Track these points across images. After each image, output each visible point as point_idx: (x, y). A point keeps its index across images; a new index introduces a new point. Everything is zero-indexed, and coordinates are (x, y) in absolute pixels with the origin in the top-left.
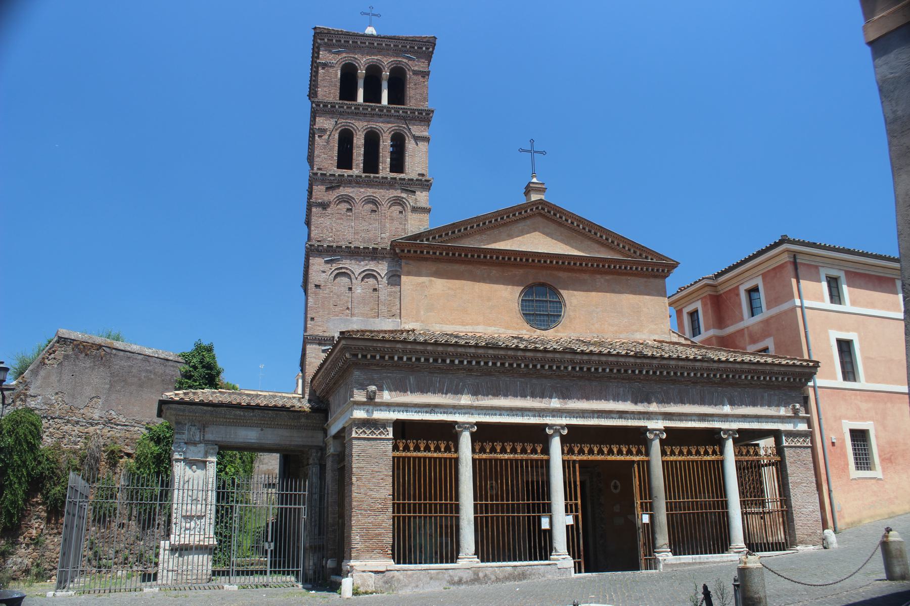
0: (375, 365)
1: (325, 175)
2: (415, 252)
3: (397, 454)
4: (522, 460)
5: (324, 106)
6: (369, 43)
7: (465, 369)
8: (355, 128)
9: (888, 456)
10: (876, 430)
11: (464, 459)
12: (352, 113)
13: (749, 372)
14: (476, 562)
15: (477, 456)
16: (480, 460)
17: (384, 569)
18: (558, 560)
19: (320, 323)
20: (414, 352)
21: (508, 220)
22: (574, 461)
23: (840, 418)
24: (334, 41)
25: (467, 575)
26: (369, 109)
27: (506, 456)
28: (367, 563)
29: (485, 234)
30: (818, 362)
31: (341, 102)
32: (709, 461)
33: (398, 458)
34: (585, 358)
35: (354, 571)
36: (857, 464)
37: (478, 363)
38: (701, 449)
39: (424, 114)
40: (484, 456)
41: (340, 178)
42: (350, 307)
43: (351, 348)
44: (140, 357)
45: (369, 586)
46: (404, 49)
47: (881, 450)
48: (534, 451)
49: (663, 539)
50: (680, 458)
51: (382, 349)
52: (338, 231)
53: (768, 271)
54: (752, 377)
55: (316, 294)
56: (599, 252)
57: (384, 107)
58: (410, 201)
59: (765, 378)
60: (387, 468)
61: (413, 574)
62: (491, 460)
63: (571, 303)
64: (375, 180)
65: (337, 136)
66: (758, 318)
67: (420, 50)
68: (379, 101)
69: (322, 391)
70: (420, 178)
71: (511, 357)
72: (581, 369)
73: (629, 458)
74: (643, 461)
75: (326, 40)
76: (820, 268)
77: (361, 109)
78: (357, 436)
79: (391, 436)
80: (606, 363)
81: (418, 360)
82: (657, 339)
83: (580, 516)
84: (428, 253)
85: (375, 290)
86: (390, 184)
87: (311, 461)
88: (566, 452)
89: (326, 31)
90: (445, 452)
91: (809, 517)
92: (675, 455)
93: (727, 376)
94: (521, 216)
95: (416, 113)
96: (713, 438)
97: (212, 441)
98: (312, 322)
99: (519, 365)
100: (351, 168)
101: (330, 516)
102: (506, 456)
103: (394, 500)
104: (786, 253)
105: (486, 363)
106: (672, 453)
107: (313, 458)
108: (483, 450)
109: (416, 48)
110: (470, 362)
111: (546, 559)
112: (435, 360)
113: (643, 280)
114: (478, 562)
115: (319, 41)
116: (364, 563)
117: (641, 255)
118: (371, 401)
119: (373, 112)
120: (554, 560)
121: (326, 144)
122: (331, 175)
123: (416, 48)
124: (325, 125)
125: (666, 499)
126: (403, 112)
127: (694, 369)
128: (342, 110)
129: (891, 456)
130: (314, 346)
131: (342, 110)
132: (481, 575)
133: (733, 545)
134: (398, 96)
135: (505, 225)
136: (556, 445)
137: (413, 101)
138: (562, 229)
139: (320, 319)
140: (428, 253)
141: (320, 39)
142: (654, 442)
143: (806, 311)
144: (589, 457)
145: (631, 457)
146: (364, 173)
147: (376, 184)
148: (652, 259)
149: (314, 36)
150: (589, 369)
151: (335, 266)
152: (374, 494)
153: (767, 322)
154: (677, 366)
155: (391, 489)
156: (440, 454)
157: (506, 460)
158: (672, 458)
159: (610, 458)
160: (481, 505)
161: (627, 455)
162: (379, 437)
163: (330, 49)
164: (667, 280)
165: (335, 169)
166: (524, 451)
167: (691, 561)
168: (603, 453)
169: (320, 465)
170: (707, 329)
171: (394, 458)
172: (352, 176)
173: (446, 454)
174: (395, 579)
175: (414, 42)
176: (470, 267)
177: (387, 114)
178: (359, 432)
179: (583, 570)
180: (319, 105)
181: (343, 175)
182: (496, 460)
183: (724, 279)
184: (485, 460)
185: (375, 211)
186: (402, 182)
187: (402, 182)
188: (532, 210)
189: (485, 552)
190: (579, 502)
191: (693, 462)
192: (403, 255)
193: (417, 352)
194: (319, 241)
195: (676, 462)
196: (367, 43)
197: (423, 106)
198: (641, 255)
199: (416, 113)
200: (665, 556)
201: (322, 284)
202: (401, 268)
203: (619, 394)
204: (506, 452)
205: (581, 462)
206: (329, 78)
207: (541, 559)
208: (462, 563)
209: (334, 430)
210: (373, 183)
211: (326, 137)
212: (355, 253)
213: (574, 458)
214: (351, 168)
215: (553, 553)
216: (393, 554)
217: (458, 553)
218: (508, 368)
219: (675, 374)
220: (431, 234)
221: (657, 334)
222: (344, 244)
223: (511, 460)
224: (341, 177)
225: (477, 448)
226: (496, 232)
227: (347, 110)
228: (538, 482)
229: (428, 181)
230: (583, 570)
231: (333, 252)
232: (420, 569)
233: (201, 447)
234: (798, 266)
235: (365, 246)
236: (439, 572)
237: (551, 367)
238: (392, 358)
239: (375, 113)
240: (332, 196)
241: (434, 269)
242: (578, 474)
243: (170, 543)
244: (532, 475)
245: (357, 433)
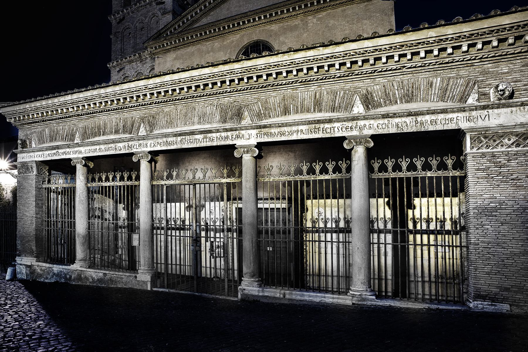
213: (163, 183)
225: (90, 178)
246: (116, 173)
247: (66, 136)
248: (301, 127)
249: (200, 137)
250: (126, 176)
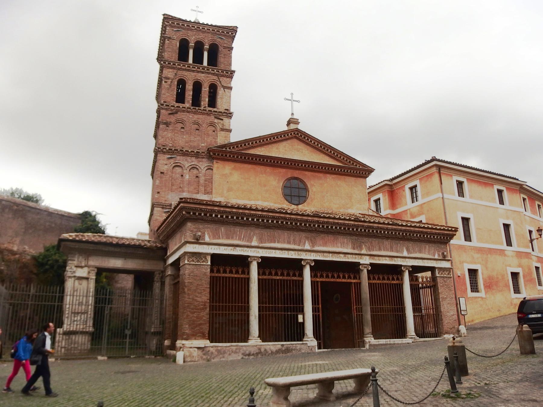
0: (201, 219)
2: (222, 155)
3: (213, 275)
4: (287, 280)
5: (169, 63)
7: (255, 224)
8: (188, 79)
9: (488, 284)
10: (482, 270)
11: (253, 279)
12: (186, 69)
13: (419, 232)
14: (259, 342)
15: (260, 277)
16: (262, 279)
17: (203, 346)
18: (308, 341)
19: (163, 196)
20: (225, 212)
21: (277, 140)
22: (317, 282)
23: (463, 262)
25: (254, 350)
26: (196, 68)
27: (278, 278)
28: (192, 342)
30: (457, 228)
31: (179, 62)
32: (395, 284)
33: (213, 277)
34: (326, 220)
35: (185, 348)
36: (471, 289)
37: (263, 220)
38: (390, 277)
40: (265, 277)
41: (177, 108)
42: (181, 186)
43: (186, 208)
44: (46, 213)
45: (193, 357)
46: (218, 33)
47: (485, 281)
48: (294, 275)
49: (368, 329)
50: (378, 282)
51: (205, 210)
52: (175, 140)
53: (423, 177)
54: (420, 236)
55: (161, 177)
56: (329, 161)
57: (205, 67)
58: (220, 125)
59: (427, 236)
60: (206, 283)
61: (221, 349)
62: (269, 279)
63: (312, 190)
64: (199, 111)
65: (176, 83)
66: (416, 204)
67: (228, 35)
68: (202, 63)
69: (164, 237)
70: (226, 111)
71: (282, 218)
72: (323, 226)
73: (349, 281)
74: (357, 283)
76: (453, 176)
78: (188, 263)
79: (209, 263)
80: (338, 223)
81: (227, 217)
82: (361, 213)
83: (321, 315)
84: (230, 156)
85: (197, 177)
86: (209, 114)
87: (155, 279)
88: (313, 276)
89: (170, 17)
90: (242, 274)
91: (451, 318)
92: (375, 280)
93: (406, 234)
94: (284, 138)
96: (396, 270)
97: (92, 266)
98: (158, 195)
99: (287, 223)
100: (184, 103)
101: (167, 313)
102: (278, 278)
103: (210, 303)
104: (435, 167)
105: (268, 221)
106: (374, 279)
107: (157, 277)
108: (264, 274)
109: (225, 32)
110: (258, 220)
111: (301, 341)
112: (237, 218)
113: (353, 179)
114: (260, 342)
115: (166, 23)
116: (191, 342)
117: (353, 164)
118: (197, 241)
119: (199, 70)
120: (306, 341)
121: (169, 87)
122: (172, 106)
123: (225, 32)
124: (169, 76)
125: (370, 306)
126: (217, 71)
127: (387, 229)
128: (179, 67)
129: (490, 284)
130: (159, 209)
131: (179, 67)
132: (262, 350)
133: (408, 334)
134: (213, 61)
136: (307, 272)
137: (223, 65)
138: (308, 147)
139: (163, 193)
140: (230, 156)
141: (167, 22)
142: (363, 272)
143: (445, 200)
144: (326, 279)
145: (350, 280)
146: (192, 106)
147: (199, 113)
148: (359, 167)
149: (163, 20)
150: (327, 227)
151: (172, 161)
152: (199, 299)
153: (421, 206)
154: (378, 228)
155: (209, 296)
156: (238, 275)
157: (278, 280)
158: (374, 282)
159: (338, 280)
160: (263, 307)
161: (348, 279)
162: (202, 264)
163: (173, 29)
164: (367, 179)
165: (175, 103)
166: (288, 275)
167: (385, 343)
168: (334, 277)
169: (161, 281)
170: (385, 210)
171: (211, 277)
172: (184, 108)
173: (242, 275)
174: (210, 352)
175: (224, 29)
176: (254, 166)
177: (207, 71)
178: (190, 261)
179: (322, 347)
180: (165, 63)
181: (179, 107)
182: (272, 280)
183: (396, 181)
184: (265, 279)
185: (198, 130)
186: (215, 113)
187: (215, 113)
188: (291, 134)
189: (264, 336)
190: (320, 306)
191: (385, 284)
192: (214, 156)
193: (227, 212)
194: (163, 146)
195: (376, 284)
196: (196, 27)
197: (228, 68)
198: (353, 164)
200: (370, 340)
201: (165, 172)
202: (213, 164)
203: (344, 242)
204: (278, 275)
205: (321, 282)
206: (172, 47)
207: (298, 341)
208: (251, 342)
209: (171, 260)
210: (197, 113)
211: (169, 83)
212: (185, 154)
213: (318, 280)
214: (184, 103)
215: (305, 337)
216: (209, 336)
217: (248, 337)
218: (281, 224)
219: (377, 231)
220: (232, 145)
221: (361, 210)
222: (179, 149)
223: (281, 280)
225: (261, 272)
227: (183, 67)
228: (296, 295)
229: (231, 113)
230: (322, 347)
231: (172, 152)
232: (225, 346)
233: (86, 270)
234: (441, 175)
235: (192, 150)
236: (237, 348)
237: (305, 225)
238: (211, 215)
240: (172, 119)
241: (233, 166)
242: (320, 289)
243: (63, 329)
244: (293, 290)
245: (188, 261)
246: (284, 270)
247: (244, 237)
248: (387, 258)
249: (342, 255)
250: (221, 270)
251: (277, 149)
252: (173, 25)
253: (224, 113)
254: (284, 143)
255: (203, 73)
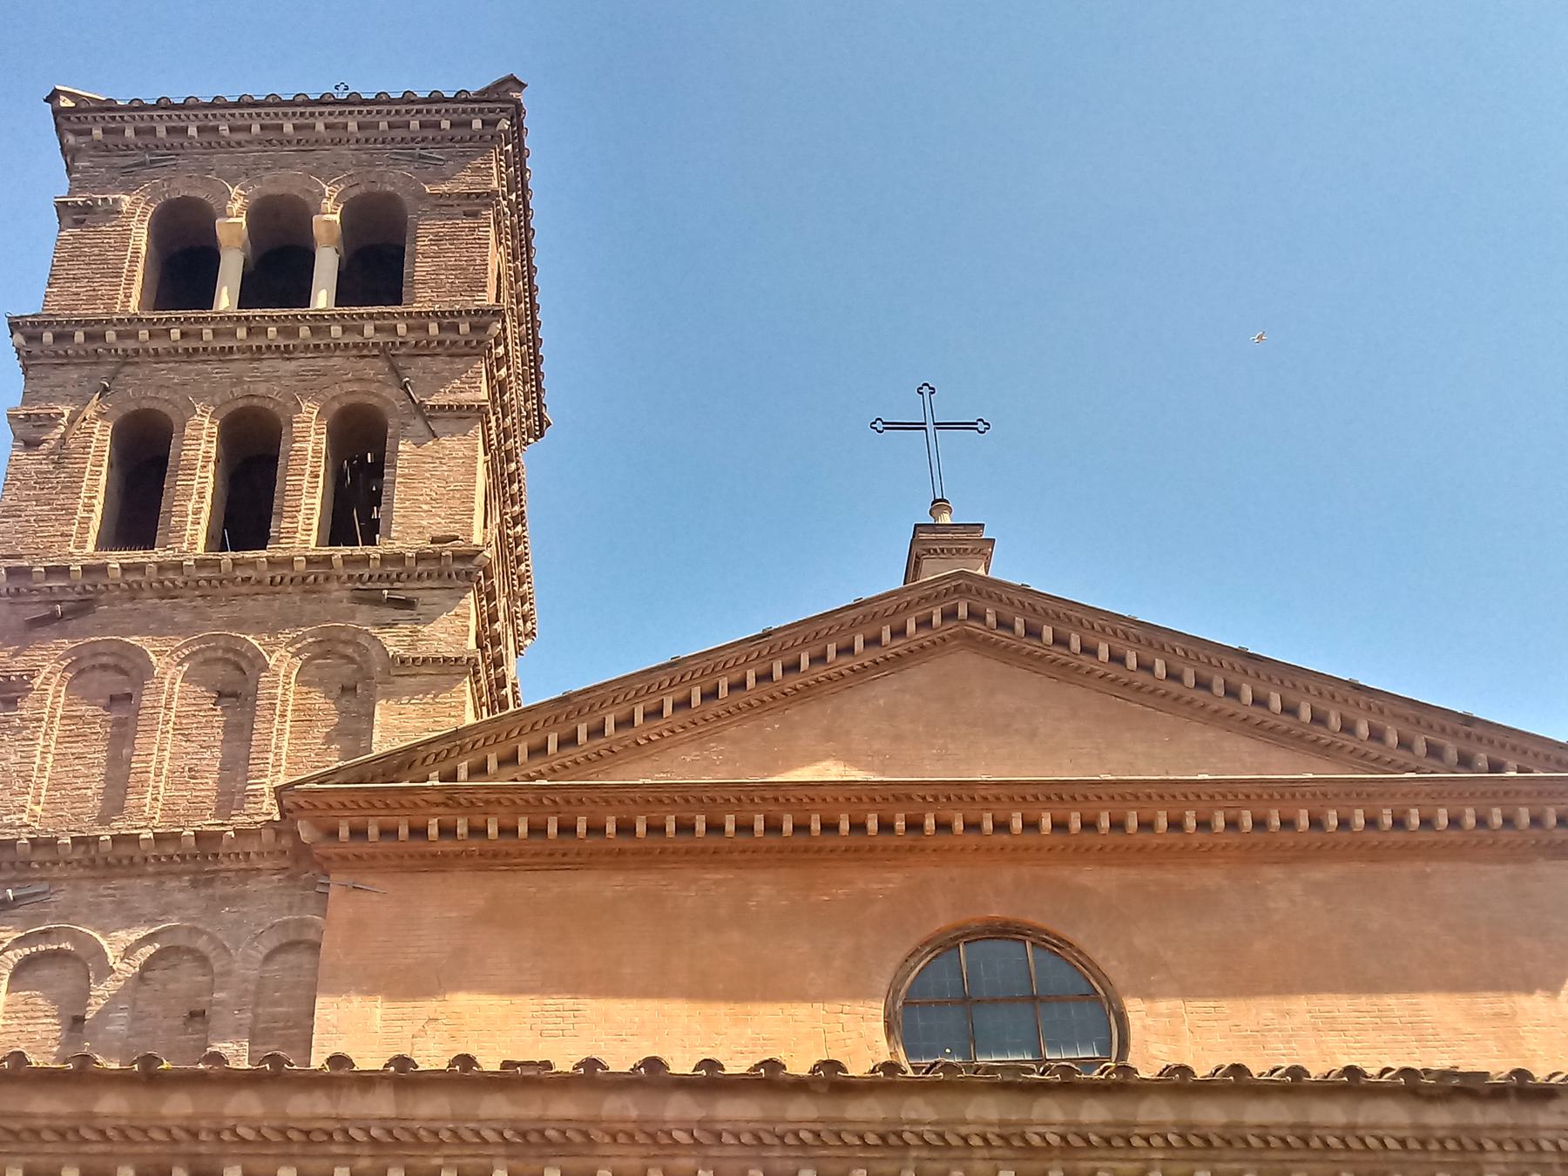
1: (26, 572)
6: (262, 127)
24: (129, 133)
29: (721, 740)
39: (464, 328)
64: (240, 573)
75: (97, 133)
77: (207, 334)
94: (876, 654)
95: (433, 328)
122: (50, 572)
135: (804, 694)
186: (357, 573)
187: (357, 573)
199: (433, 328)
224: (94, 578)
226: (772, 725)
239: (262, 342)
251: (828, 735)
252: (111, 140)
253: (421, 557)
254: (882, 692)
255: (286, 353)
